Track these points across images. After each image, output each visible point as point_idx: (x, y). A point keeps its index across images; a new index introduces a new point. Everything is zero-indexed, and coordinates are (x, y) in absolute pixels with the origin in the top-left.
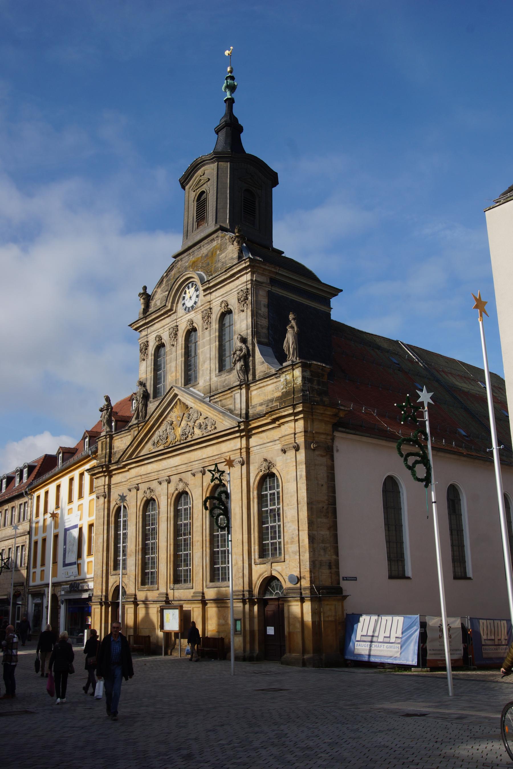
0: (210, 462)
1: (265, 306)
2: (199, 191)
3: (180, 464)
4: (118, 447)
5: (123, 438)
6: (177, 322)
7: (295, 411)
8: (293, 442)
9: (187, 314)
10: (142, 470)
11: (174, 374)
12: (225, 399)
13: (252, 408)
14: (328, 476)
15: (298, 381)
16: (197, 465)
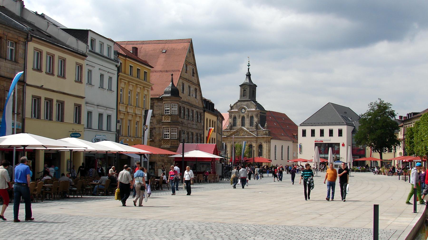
2: (244, 89)
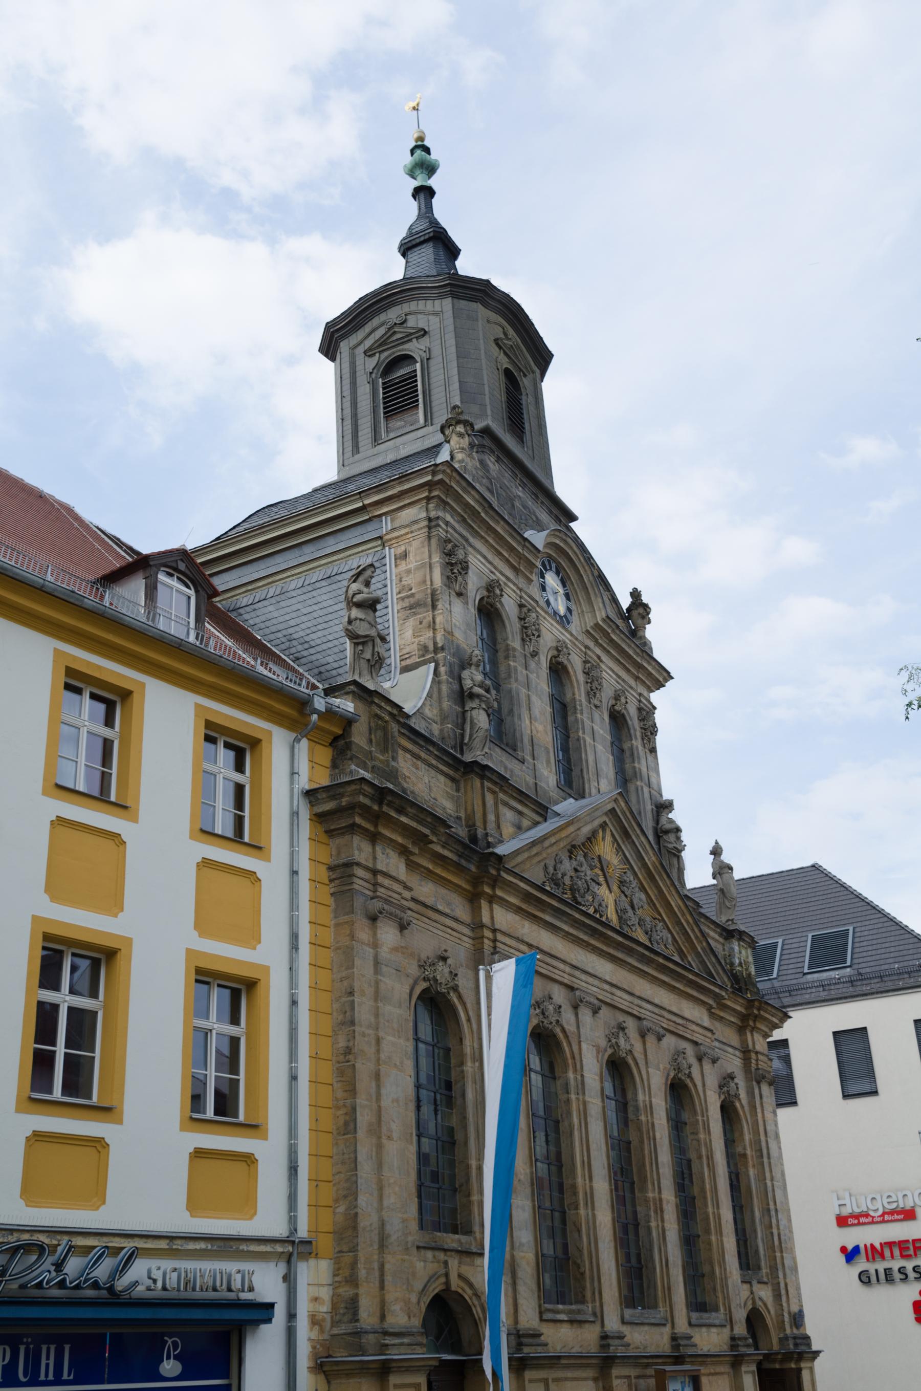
5: (419, 763)
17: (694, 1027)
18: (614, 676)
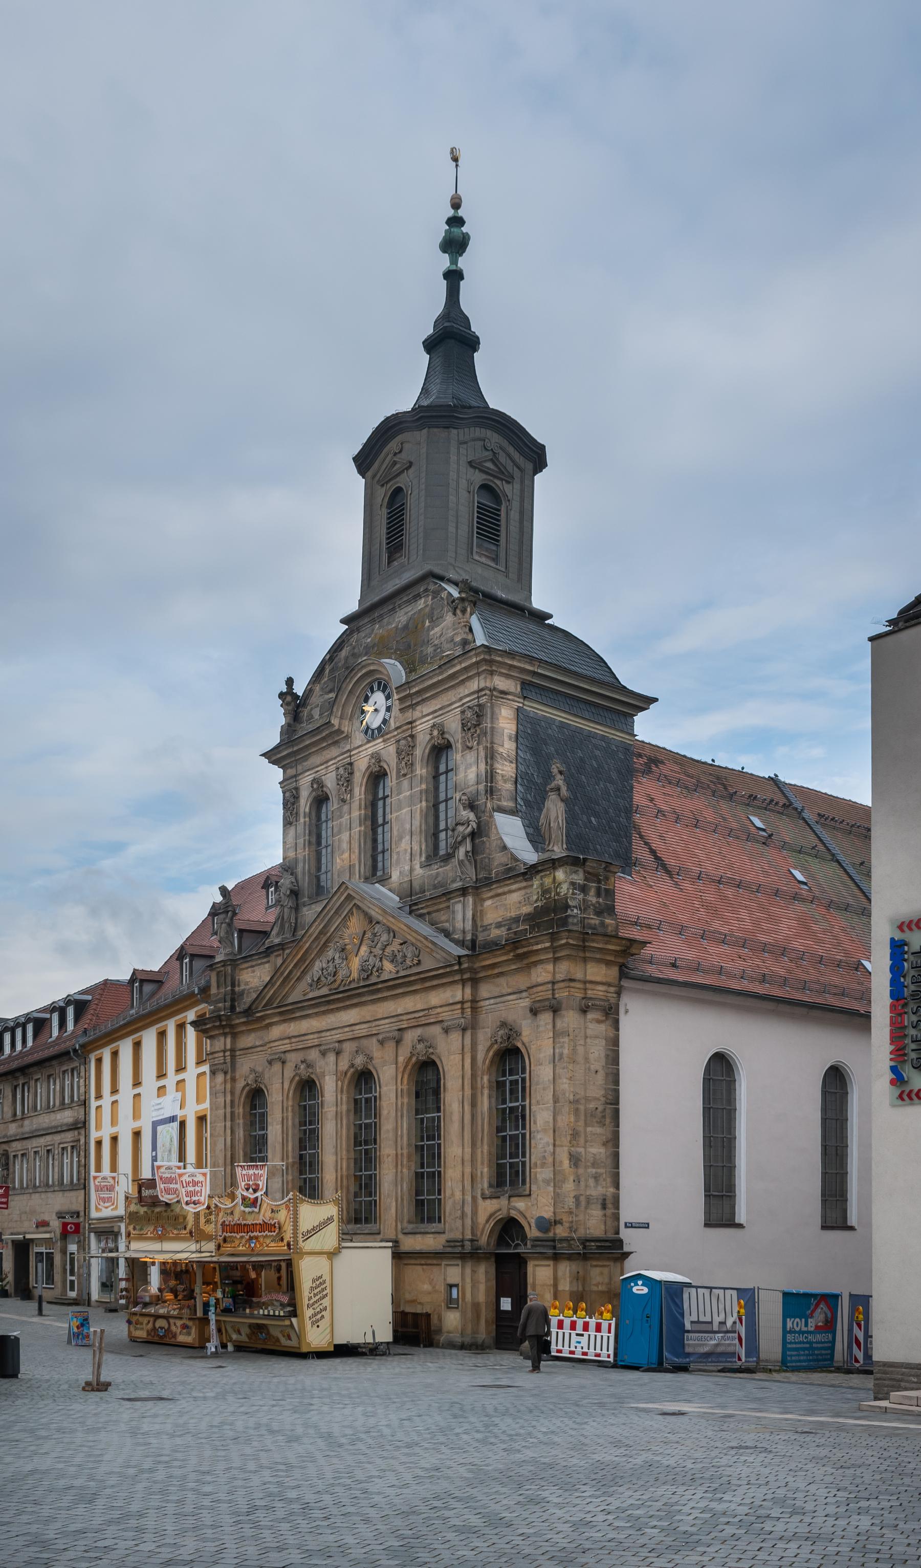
0: (410, 1021)
1: (510, 739)
3: (358, 1021)
4: (247, 983)
6: (350, 756)
7: (555, 944)
8: (550, 996)
9: (369, 742)
10: (292, 1028)
11: (346, 855)
12: (438, 911)
13: (484, 931)
14: (607, 1056)
15: (562, 890)
16: (387, 1026)
17: (439, 1010)
18: (431, 717)
